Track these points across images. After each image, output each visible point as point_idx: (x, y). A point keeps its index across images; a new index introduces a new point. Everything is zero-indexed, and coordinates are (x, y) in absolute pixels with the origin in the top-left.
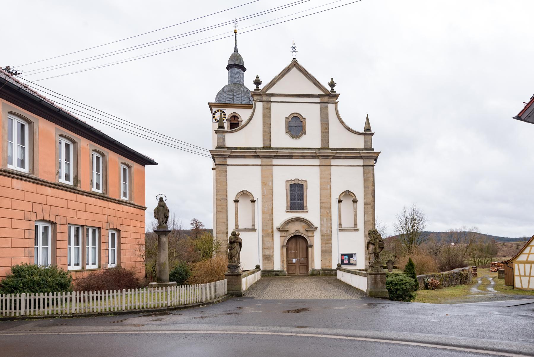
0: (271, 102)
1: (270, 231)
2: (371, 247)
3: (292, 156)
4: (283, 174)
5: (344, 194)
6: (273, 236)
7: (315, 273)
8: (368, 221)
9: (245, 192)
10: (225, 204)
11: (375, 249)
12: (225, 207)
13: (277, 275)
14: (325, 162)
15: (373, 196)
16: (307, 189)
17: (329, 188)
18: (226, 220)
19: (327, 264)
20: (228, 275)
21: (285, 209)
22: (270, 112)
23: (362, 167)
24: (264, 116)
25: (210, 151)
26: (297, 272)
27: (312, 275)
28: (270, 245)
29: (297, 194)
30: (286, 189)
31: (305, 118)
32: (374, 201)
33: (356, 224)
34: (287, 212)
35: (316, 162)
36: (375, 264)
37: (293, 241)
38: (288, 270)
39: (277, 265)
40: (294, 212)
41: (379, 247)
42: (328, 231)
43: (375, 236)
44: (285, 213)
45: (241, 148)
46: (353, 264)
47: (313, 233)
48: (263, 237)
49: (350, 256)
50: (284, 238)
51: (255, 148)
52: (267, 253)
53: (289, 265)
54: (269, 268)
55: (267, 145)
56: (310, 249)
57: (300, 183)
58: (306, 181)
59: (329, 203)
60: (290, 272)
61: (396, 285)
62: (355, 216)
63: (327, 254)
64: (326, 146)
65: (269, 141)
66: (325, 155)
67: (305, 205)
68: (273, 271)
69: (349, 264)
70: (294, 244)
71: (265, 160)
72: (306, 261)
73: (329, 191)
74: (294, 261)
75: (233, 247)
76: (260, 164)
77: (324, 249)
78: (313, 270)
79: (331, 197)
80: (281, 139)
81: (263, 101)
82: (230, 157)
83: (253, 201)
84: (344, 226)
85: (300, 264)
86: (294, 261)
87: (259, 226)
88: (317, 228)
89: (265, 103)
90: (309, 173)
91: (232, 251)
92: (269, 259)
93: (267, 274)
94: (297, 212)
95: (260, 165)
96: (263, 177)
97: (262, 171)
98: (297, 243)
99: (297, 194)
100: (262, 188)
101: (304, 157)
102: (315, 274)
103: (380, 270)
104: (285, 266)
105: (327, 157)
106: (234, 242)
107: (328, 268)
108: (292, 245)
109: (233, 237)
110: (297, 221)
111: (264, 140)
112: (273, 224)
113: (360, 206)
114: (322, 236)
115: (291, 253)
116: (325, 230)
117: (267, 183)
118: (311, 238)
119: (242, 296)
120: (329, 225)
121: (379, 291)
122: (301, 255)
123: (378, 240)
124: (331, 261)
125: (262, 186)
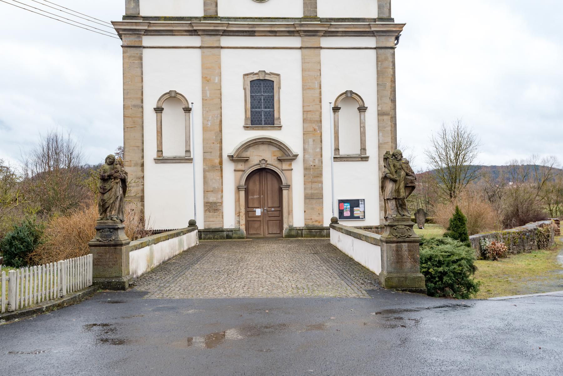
1: (217, 161)
2: (390, 186)
4: (240, 62)
5: (344, 96)
6: (222, 170)
7: (293, 233)
8: (385, 143)
9: (173, 95)
10: (140, 115)
11: (398, 191)
12: (140, 120)
13: (228, 237)
15: (394, 101)
16: (279, 88)
17: (317, 86)
18: (140, 142)
19: (315, 217)
20: (95, 246)
21: (242, 123)
25: (113, 23)
26: (264, 231)
27: (289, 236)
28: (216, 185)
29: (262, 96)
30: (245, 89)
32: (395, 109)
34: (246, 128)
36: (398, 220)
37: (256, 177)
38: (247, 229)
39: (230, 219)
41: (406, 187)
42: (317, 161)
43: (398, 164)
44: (243, 129)
45: (166, 18)
46: (358, 217)
47: (291, 165)
48: (205, 171)
49: (355, 203)
50: (241, 173)
51: (190, 18)
52: (212, 199)
53: (250, 219)
54: (214, 225)
56: (285, 192)
57: (267, 78)
58: (278, 75)
59: (318, 113)
60: (252, 232)
61: (440, 264)
67: (276, 116)
68: (223, 231)
69: (352, 217)
70: (257, 183)
71: (207, 38)
72: (278, 213)
73: (318, 91)
74: (258, 212)
75: (108, 186)
76: (199, 45)
77: (309, 192)
78: (291, 229)
79: (321, 102)
84: (343, 152)
85: (268, 218)
86: (258, 212)
87: (197, 153)
88: (297, 156)
90: (283, 61)
91: (106, 196)
92: (216, 210)
93: (211, 236)
94: (263, 128)
95: (200, 48)
96: (204, 67)
97: (203, 58)
98: (264, 182)
99: (262, 96)
100: (203, 87)
102: (295, 234)
103: (407, 234)
104: (243, 222)
106: (110, 177)
107: (317, 224)
108: (255, 186)
109: (107, 167)
112: (221, 149)
114: (306, 169)
115: (253, 199)
116: (311, 159)
117: (211, 79)
119: (123, 288)
120: (318, 150)
121: (406, 278)
122: (270, 203)
123: (403, 173)
124: (321, 213)
125: (203, 83)
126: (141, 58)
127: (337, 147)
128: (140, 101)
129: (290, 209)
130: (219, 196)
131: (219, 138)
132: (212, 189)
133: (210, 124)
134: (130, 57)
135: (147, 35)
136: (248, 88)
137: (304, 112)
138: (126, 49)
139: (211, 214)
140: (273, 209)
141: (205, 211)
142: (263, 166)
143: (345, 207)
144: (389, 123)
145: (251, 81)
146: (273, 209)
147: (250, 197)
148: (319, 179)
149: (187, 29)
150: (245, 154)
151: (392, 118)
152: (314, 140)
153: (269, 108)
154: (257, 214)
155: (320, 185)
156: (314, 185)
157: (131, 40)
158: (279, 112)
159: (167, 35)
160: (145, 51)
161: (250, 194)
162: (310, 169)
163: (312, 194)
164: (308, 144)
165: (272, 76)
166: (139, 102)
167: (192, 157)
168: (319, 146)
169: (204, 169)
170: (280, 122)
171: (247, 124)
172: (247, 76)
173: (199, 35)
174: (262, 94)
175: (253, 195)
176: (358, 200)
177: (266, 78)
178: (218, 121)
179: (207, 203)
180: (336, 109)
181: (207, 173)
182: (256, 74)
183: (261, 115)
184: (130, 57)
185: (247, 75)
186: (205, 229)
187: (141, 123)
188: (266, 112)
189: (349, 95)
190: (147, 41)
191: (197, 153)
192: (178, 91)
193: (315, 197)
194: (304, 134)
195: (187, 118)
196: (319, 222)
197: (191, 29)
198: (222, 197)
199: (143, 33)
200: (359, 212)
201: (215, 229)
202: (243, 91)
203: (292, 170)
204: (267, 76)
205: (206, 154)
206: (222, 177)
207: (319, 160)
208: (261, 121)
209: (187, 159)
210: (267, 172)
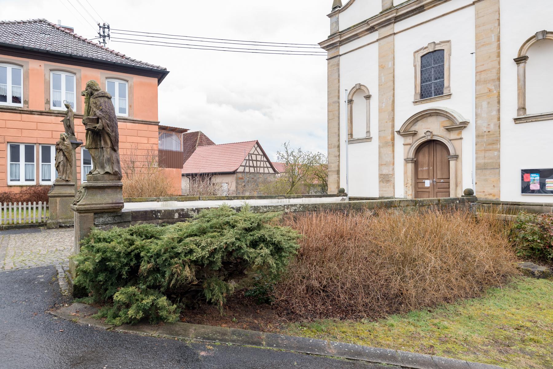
1: (389, 137)
3: (423, 6)
6: (393, 145)
9: (358, 87)
16: (450, 55)
17: (494, 39)
28: (389, 159)
30: (415, 66)
37: (426, 150)
42: (492, 126)
47: (460, 133)
48: (380, 147)
50: (409, 146)
52: (385, 172)
56: (452, 163)
59: (495, 71)
63: (488, 172)
67: (446, 84)
70: (427, 155)
73: (495, 45)
74: (427, 183)
77: (482, 161)
82: (342, 43)
86: (427, 183)
87: (375, 133)
92: (388, 181)
96: (381, 56)
108: (424, 158)
110: (430, 115)
114: (478, 136)
115: (422, 171)
118: (456, 143)
120: (494, 113)
126: (338, 65)
128: (337, 98)
129: (459, 180)
130: (391, 169)
131: (391, 117)
134: (332, 66)
135: (342, 45)
137: (477, 73)
140: (442, 181)
141: (380, 182)
142: (429, 138)
143: (532, 178)
145: (422, 57)
146: (442, 181)
147: (420, 169)
148: (495, 146)
149: (366, 28)
150: (414, 128)
152: (489, 103)
153: (439, 78)
155: (496, 153)
156: (488, 154)
157: (333, 52)
159: (355, 39)
161: (419, 166)
162: (483, 136)
165: (443, 44)
166: (336, 99)
167: (371, 136)
168: (497, 108)
173: (377, 30)
174: (433, 66)
175: (422, 167)
177: (436, 49)
178: (391, 101)
181: (381, 149)
182: (426, 48)
183: (431, 88)
185: (417, 51)
188: (436, 83)
189: (540, 37)
190: (343, 49)
191: (375, 133)
192: (362, 84)
194: (476, 98)
195: (368, 104)
196: (494, 196)
197: (369, 27)
198: (393, 169)
202: (414, 68)
203: (461, 139)
206: (393, 151)
208: (431, 93)
209: (368, 139)
210: (436, 144)
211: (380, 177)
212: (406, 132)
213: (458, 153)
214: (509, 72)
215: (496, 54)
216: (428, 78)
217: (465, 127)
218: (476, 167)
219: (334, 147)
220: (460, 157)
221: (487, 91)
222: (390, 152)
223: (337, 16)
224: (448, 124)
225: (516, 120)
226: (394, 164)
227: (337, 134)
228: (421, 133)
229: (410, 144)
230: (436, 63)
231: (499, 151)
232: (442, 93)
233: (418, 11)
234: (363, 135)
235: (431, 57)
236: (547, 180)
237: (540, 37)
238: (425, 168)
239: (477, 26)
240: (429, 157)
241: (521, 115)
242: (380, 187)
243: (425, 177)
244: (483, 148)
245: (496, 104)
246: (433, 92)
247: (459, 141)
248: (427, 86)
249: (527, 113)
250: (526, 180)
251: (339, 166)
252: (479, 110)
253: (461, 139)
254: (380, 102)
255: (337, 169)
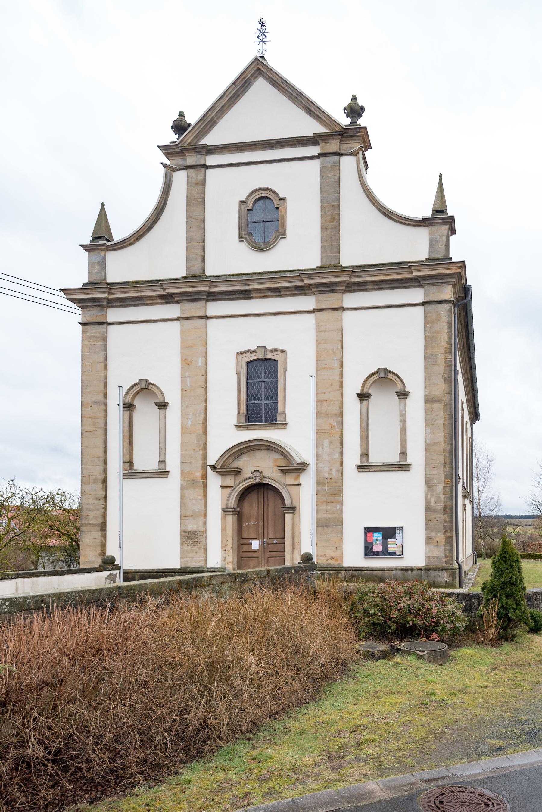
0: (207, 167)
1: (199, 474)
4: (233, 335)
5: (375, 377)
6: (205, 487)
8: (434, 444)
9: (143, 385)
14: (330, 300)
16: (285, 370)
17: (336, 364)
19: (331, 553)
21: (234, 421)
22: (204, 192)
23: (421, 309)
24: (190, 202)
28: (197, 507)
30: (238, 374)
31: (283, 200)
33: (367, 455)
34: (238, 427)
35: (308, 302)
37: (253, 497)
39: (217, 555)
40: (255, 428)
42: (334, 472)
46: (394, 554)
47: (298, 477)
48: (182, 488)
49: (389, 533)
50: (229, 490)
52: (191, 526)
54: (193, 564)
55: (196, 271)
56: (288, 517)
57: (269, 356)
58: (283, 351)
59: (337, 403)
62: (403, 431)
63: (330, 530)
64: (333, 263)
65: (199, 260)
66: (332, 282)
67: (280, 409)
69: (385, 553)
70: (255, 505)
73: (338, 371)
74: (256, 545)
77: (323, 516)
79: (341, 386)
80: (229, 256)
81: (186, 168)
83: (163, 405)
84: (375, 459)
85: (268, 554)
86: (256, 545)
87: (174, 464)
89: (191, 171)
90: (288, 331)
92: (196, 542)
95: (179, 319)
96: (185, 346)
97: (183, 332)
98: (259, 501)
100: (182, 373)
101: (277, 292)
105: (330, 288)
107: (333, 563)
108: (251, 508)
111: (188, 260)
113: (416, 405)
114: (318, 483)
116: (327, 469)
118: (293, 490)
120: (337, 456)
124: (339, 546)
126: (105, 339)
127: (365, 451)
129: (296, 540)
130: (201, 523)
131: (202, 443)
132: (191, 514)
133: (190, 423)
134: (90, 337)
136: (243, 372)
137: (317, 401)
138: (86, 327)
139: (189, 547)
140: (275, 541)
141: (182, 543)
142: (258, 480)
143: (375, 538)
144: (442, 414)
145: (248, 363)
146: (275, 541)
147: (245, 524)
148: (337, 498)
150: (237, 464)
151: (445, 405)
152: (330, 442)
153: (272, 399)
154: (253, 548)
155: (338, 506)
156: (330, 507)
157: (94, 315)
158: (284, 404)
160: (111, 328)
161: (244, 519)
162: (324, 484)
163: (327, 520)
164: (322, 448)
165: (276, 353)
166: (100, 397)
167: (167, 469)
168: (338, 450)
169: (181, 485)
170: (285, 418)
171: (240, 422)
172: (241, 356)
173: (177, 302)
175: (249, 521)
176: (395, 528)
177: (268, 357)
179: (184, 532)
180: (128, 407)
181: (185, 491)
182: (254, 352)
183: (261, 410)
184: (90, 337)
186: (181, 568)
187: (102, 425)
188: (267, 405)
189: (382, 375)
190: (113, 315)
191: (174, 464)
192: (151, 381)
193: (331, 524)
194: (317, 434)
196: (336, 560)
198: (205, 523)
199: (105, 303)
200: (395, 546)
201: (194, 568)
202: (236, 376)
203: (299, 485)
204: (268, 353)
205: (184, 464)
206: (205, 496)
207: (337, 471)
208: (261, 417)
209: (163, 473)
210: (268, 489)
211: (182, 536)
212: (226, 468)
213: (295, 505)
214: (352, 408)
215: (339, 383)
216: (257, 395)
217: (304, 470)
218: (317, 523)
219: (95, 481)
220: (297, 509)
221: (328, 427)
222: (200, 498)
223: (102, 253)
224: (282, 463)
225: (359, 467)
226: (205, 516)
227: (102, 459)
228: (247, 472)
229: (231, 487)
230: (268, 377)
231: (342, 504)
232: (276, 421)
233: (242, 296)
234: (154, 466)
235: (261, 366)
236: (389, 540)
237: (382, 375)
238: (253, 523)
239: (318, 342)
240: (258, 507)
241: (364, 462)
242: (183, 552)
243: (253, 535)
244: (324, 499)
245: (339, 445)
246: (263, 415)
247: (297, 487)
248: (255, 406)
249: (370, 461)
250: (369, 540)
251: (104, 516)
252: (320, 450)
253: (299, 485)
254: (183, 416)
255: (100, 521)
